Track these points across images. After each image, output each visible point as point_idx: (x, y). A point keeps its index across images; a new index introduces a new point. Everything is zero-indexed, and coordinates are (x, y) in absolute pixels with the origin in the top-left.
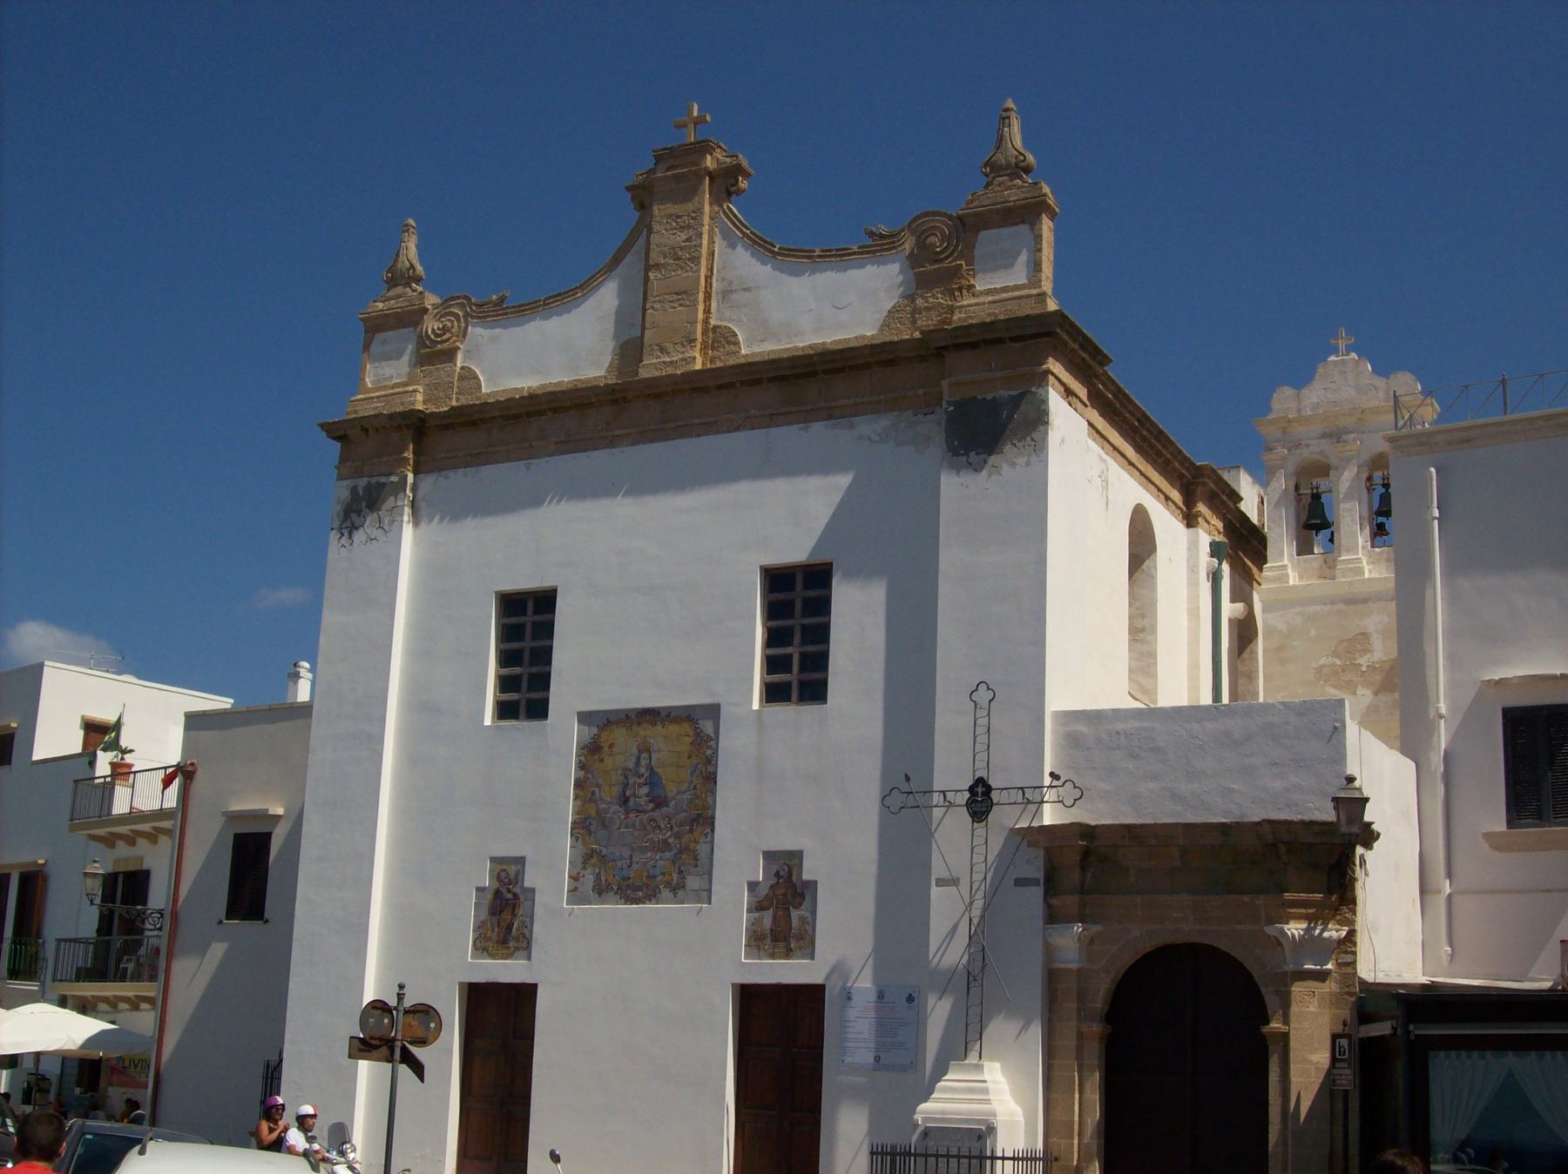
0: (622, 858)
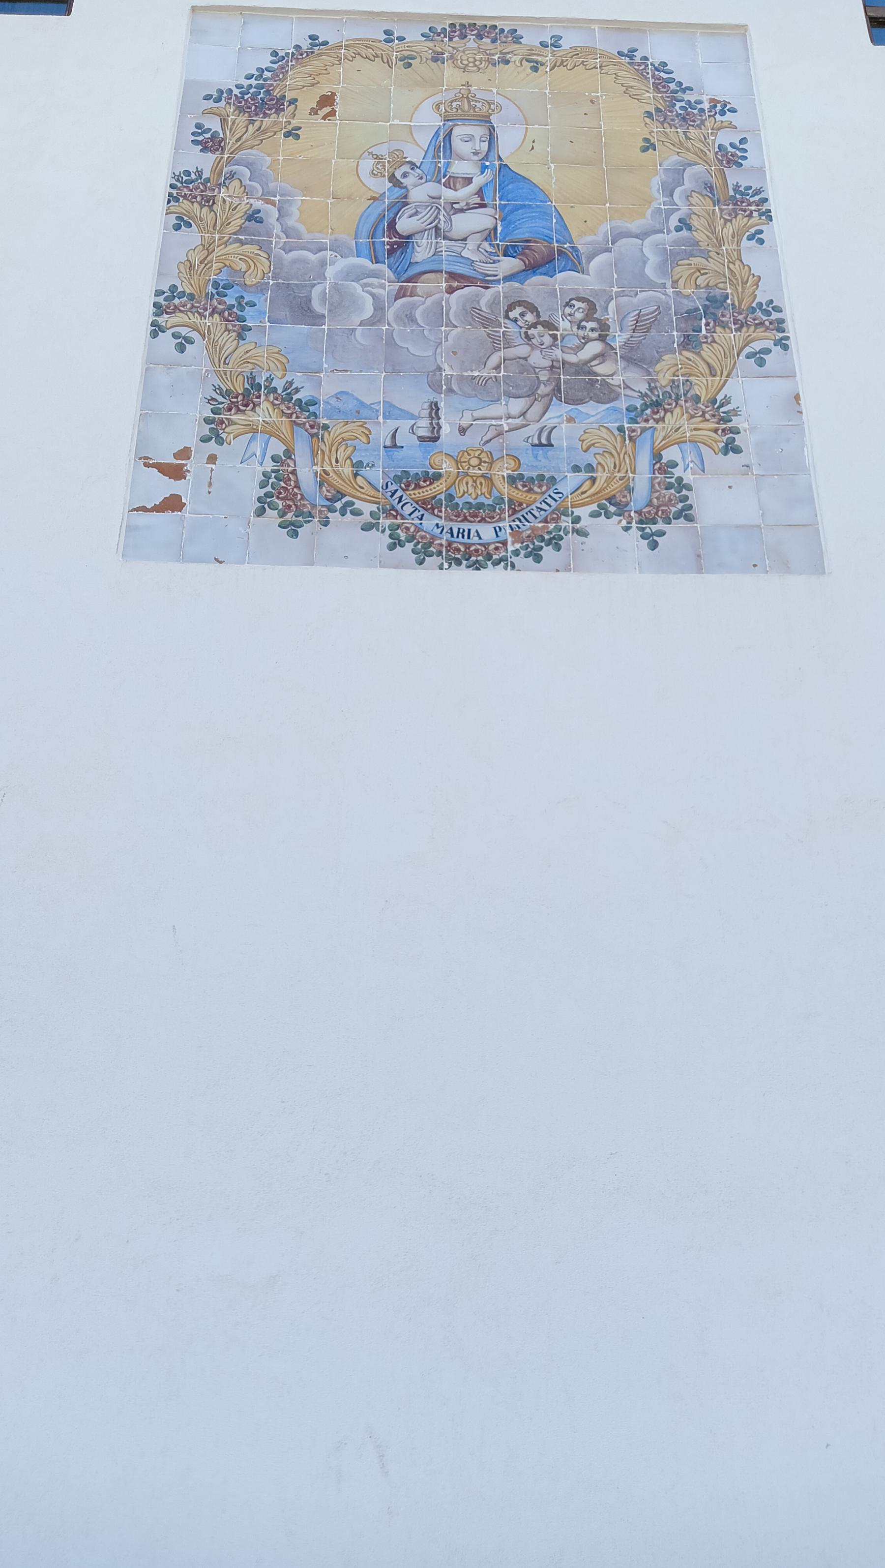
0: (391, 411)
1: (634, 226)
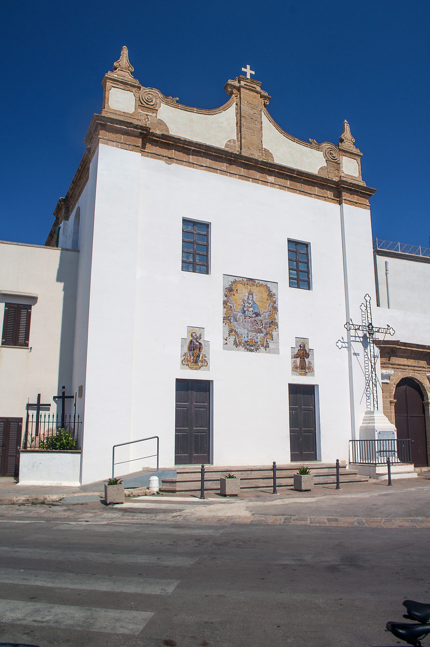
1: (266, 311)
